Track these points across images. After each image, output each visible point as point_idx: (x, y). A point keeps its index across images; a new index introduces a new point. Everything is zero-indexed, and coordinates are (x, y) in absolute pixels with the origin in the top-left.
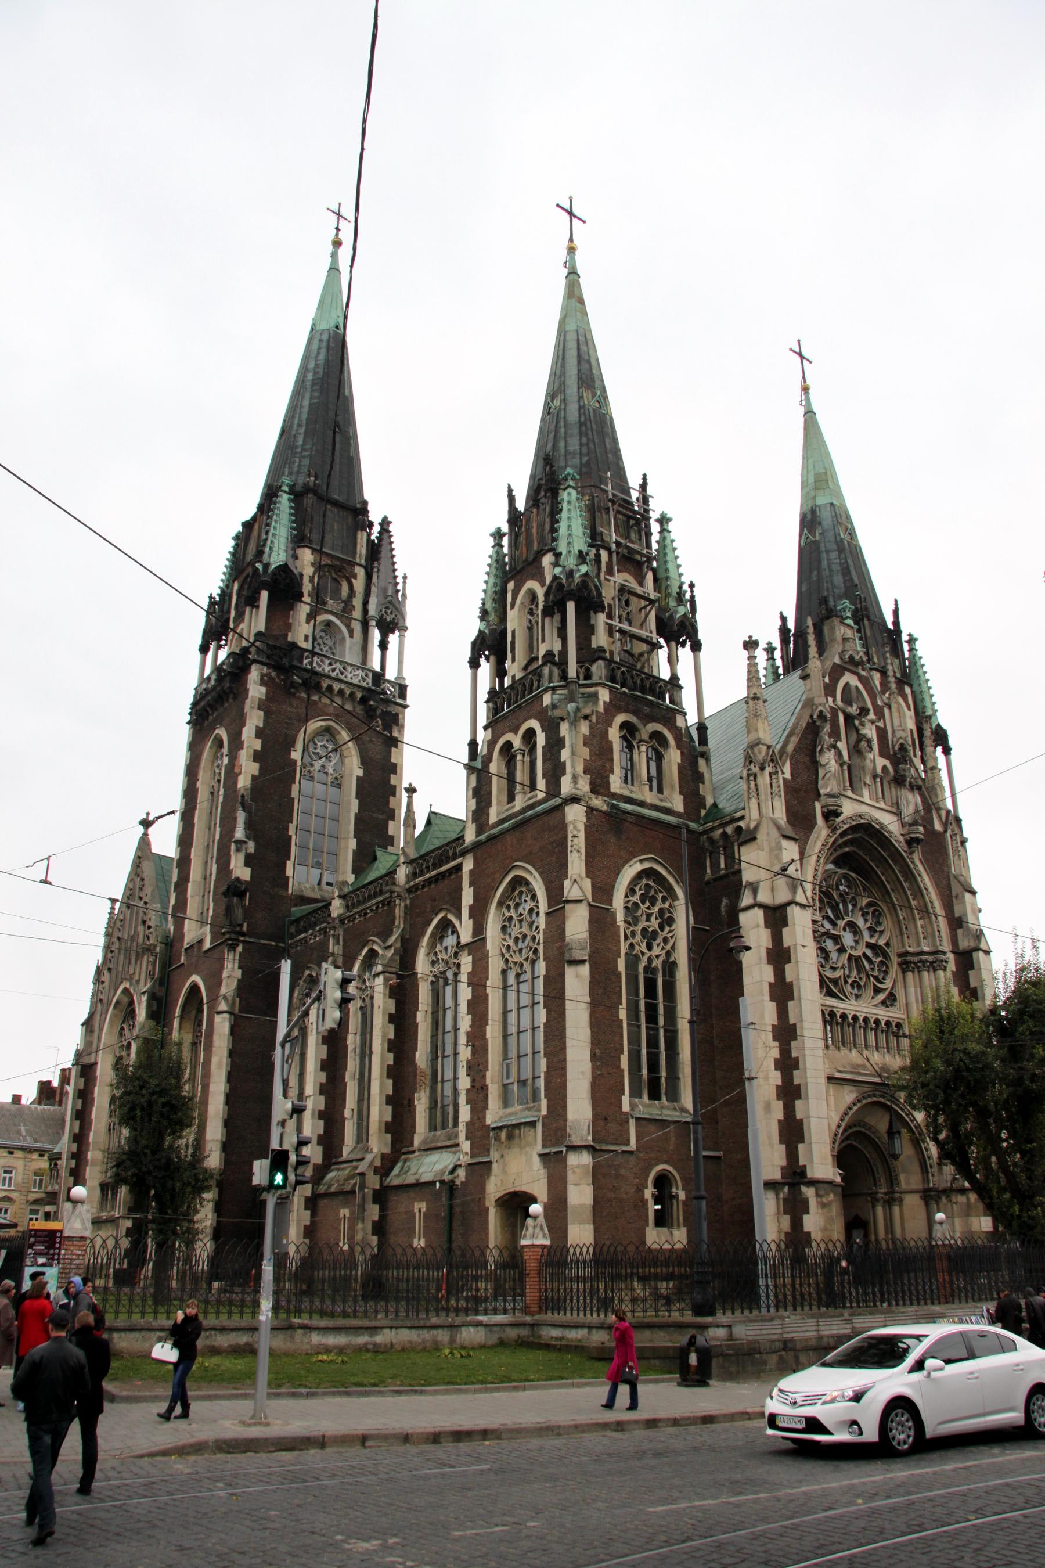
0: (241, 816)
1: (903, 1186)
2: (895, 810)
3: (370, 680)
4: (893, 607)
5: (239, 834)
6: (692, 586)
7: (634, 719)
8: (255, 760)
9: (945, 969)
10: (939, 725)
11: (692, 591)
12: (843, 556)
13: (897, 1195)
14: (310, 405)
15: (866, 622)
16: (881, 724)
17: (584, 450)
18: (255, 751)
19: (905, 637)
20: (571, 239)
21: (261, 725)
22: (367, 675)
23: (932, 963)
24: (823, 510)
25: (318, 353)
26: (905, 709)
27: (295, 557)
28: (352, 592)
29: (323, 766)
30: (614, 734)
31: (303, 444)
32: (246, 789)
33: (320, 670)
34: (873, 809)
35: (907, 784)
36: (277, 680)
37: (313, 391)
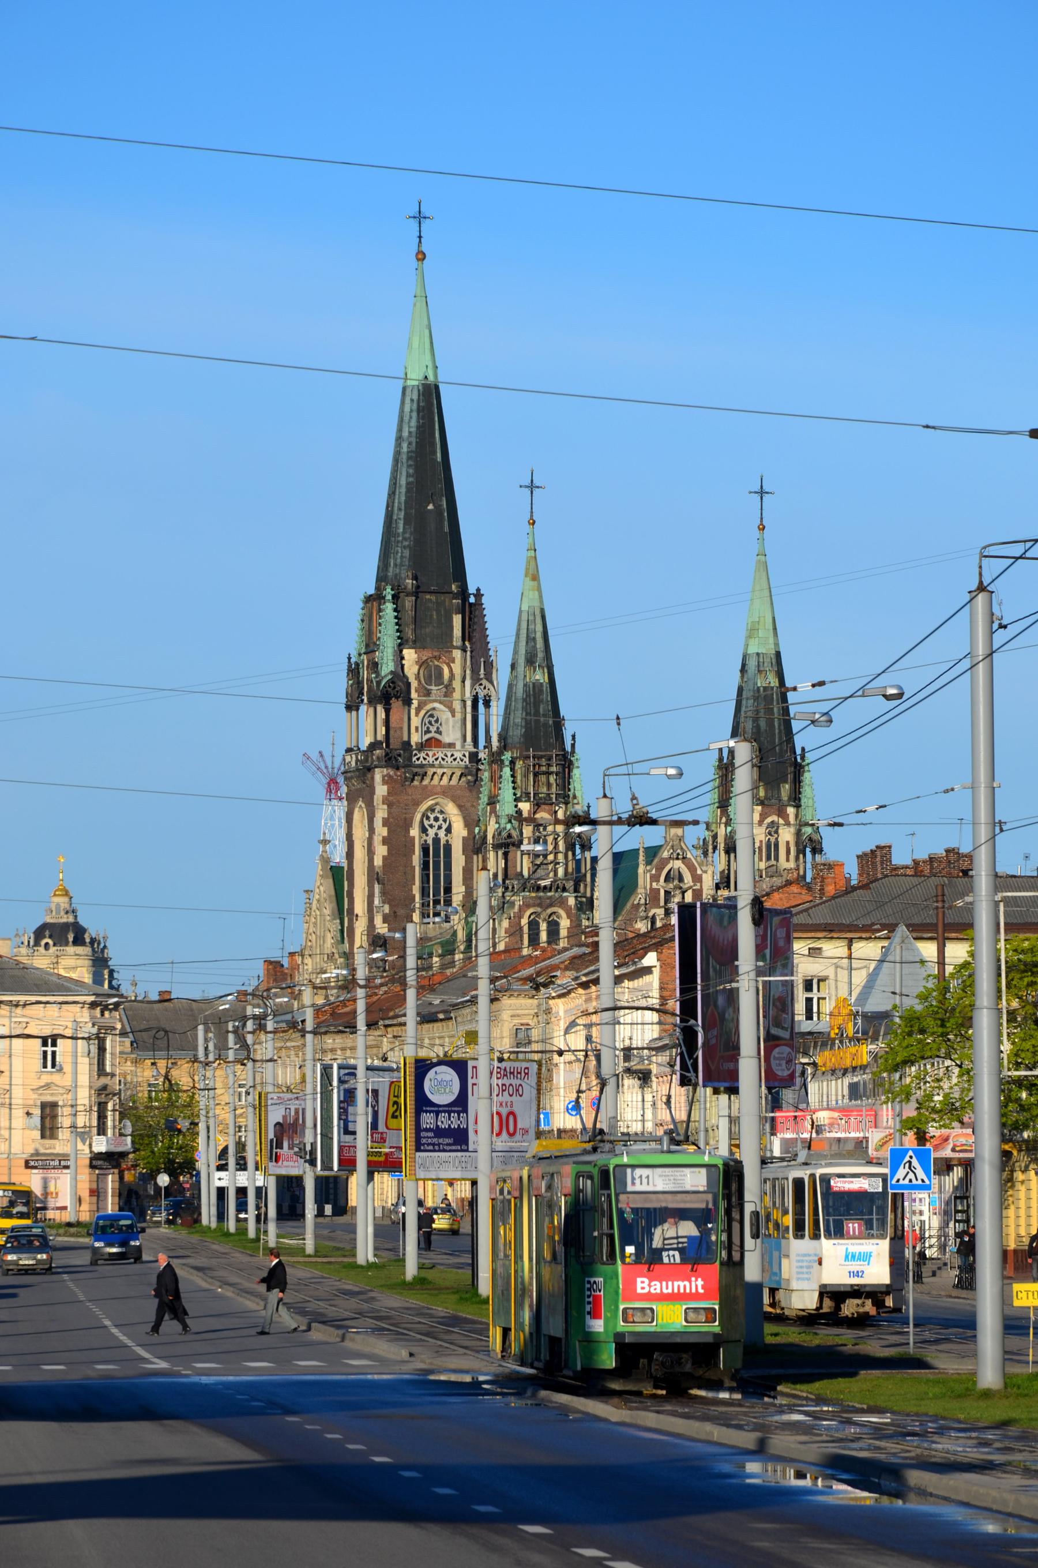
0: (377, 888)
3: (467, 760)
5: (376, 902)
7: (539, 910)
8: (383, 844)
14: (408, 484)
16: (698, 887)
17: (523, 724)
18: (383, 837)
20: (532, 516)
21: (386, 816)
22: (464, 755)
25: (411, 417)
27: (402, 658)
28: (452, 676)
29: (436, 834)
30: (524, 921)
31: (404, 532)
32: (380, 867)
33: (424, 762)
36: (395, 777)
37: (409, 466)
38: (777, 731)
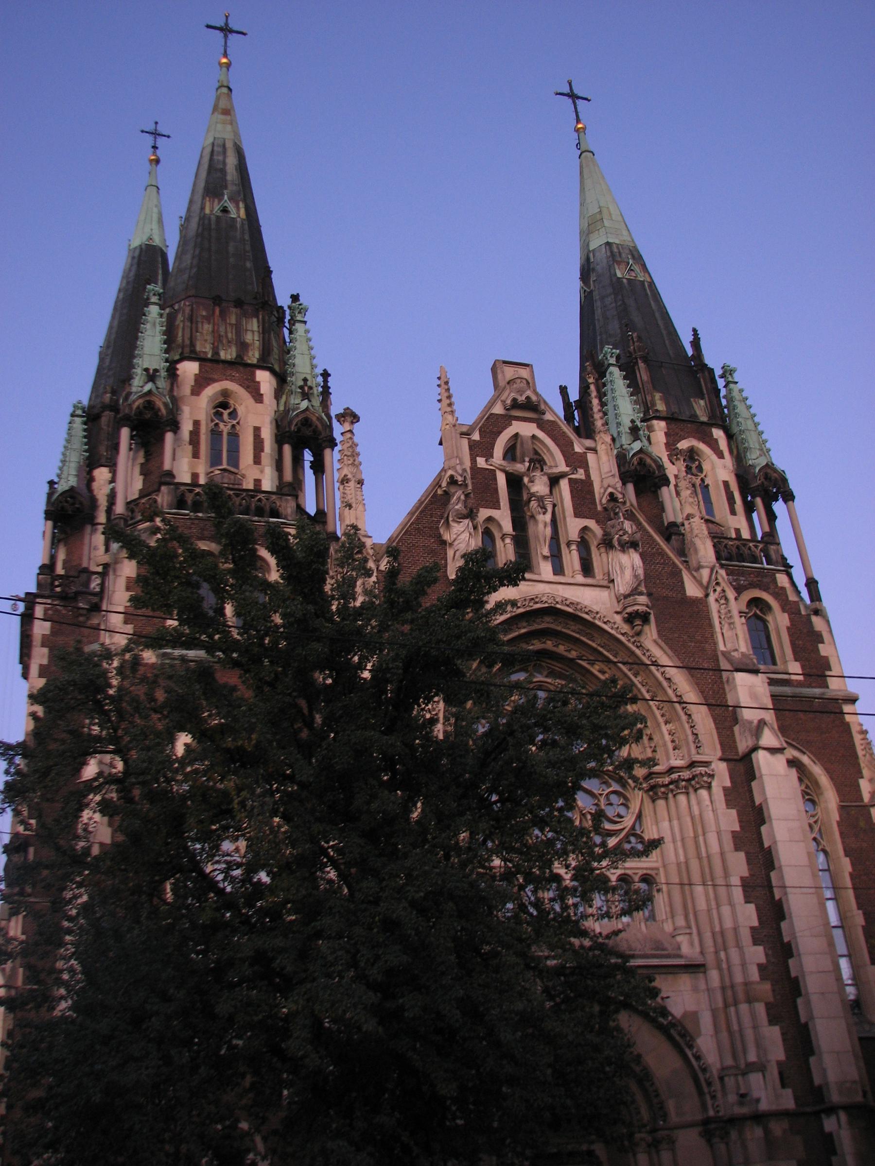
1: (674, 1118)
2: (605, 583)
4: (691, 338)
6: (326, 375)
9: (709, 787)
10: (769, 466)
11: (326, 381)
12: (620, 297)
13: (660, 1134)
15: (641, 365)
16: (580, 475)
19: (718, 372)
23: (689, 780)
24: (597, 254)
26: (714, 457)
34: (560, 587)
35: (616, 543)
38: (664, 332)
